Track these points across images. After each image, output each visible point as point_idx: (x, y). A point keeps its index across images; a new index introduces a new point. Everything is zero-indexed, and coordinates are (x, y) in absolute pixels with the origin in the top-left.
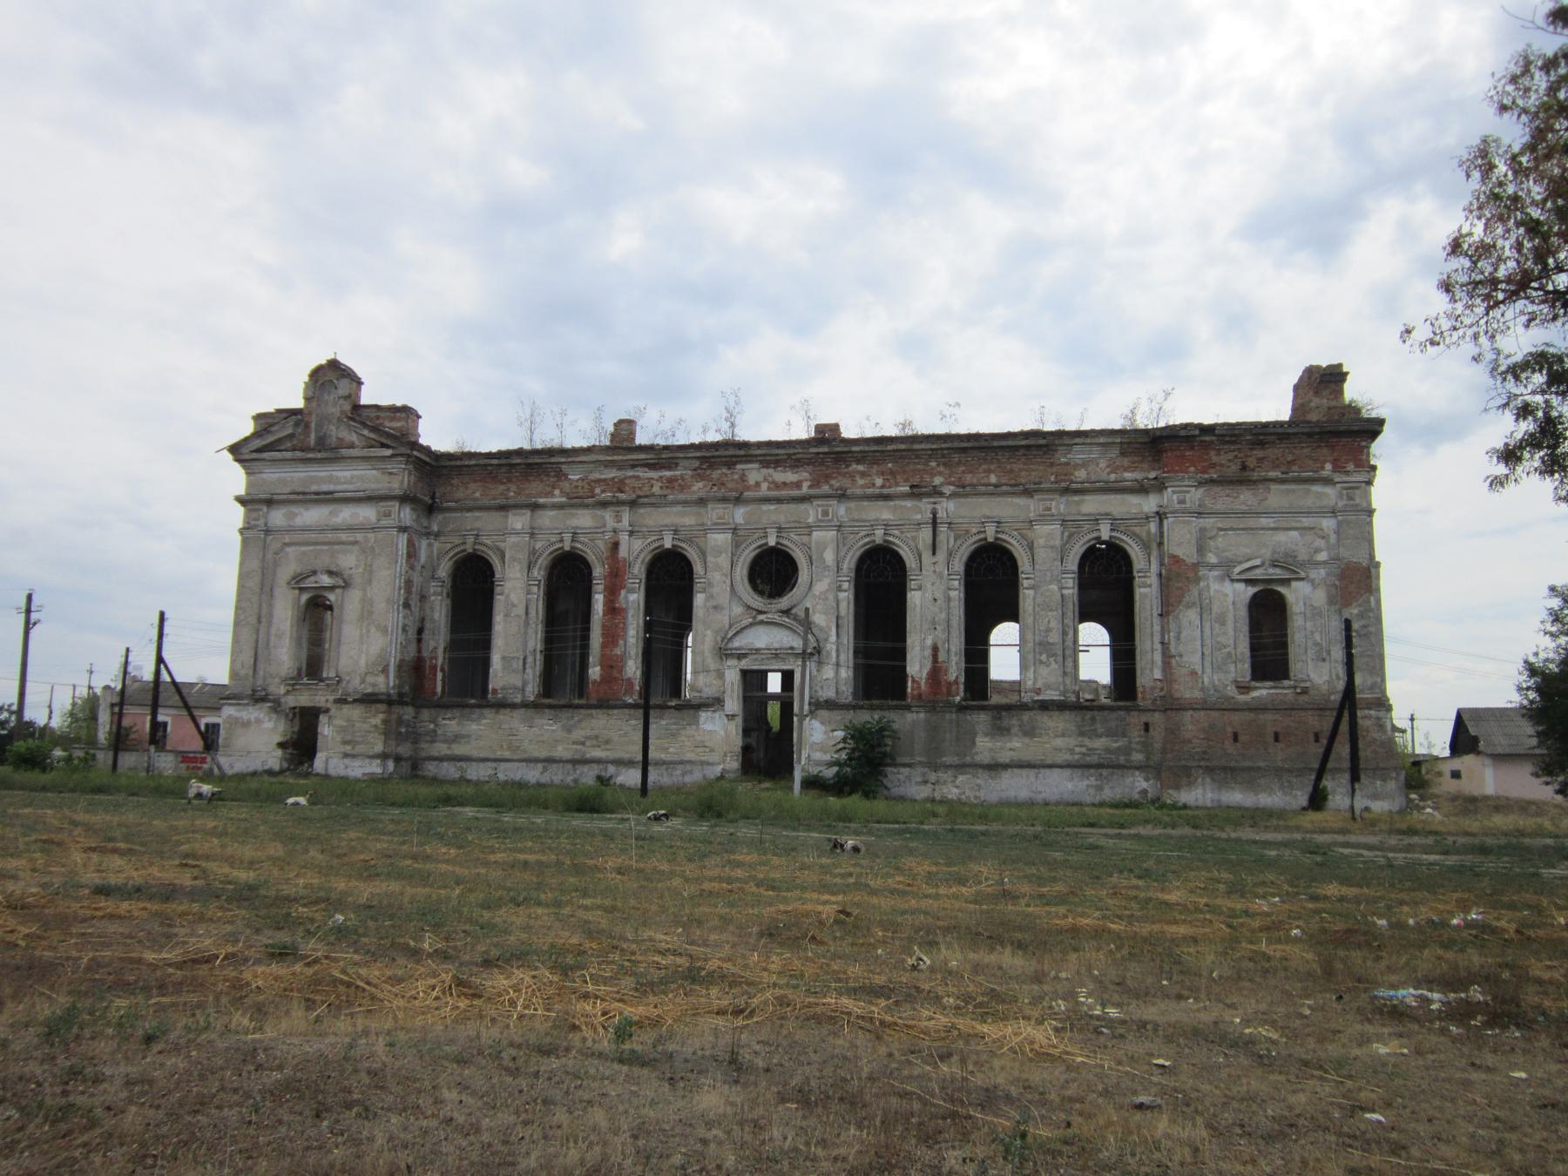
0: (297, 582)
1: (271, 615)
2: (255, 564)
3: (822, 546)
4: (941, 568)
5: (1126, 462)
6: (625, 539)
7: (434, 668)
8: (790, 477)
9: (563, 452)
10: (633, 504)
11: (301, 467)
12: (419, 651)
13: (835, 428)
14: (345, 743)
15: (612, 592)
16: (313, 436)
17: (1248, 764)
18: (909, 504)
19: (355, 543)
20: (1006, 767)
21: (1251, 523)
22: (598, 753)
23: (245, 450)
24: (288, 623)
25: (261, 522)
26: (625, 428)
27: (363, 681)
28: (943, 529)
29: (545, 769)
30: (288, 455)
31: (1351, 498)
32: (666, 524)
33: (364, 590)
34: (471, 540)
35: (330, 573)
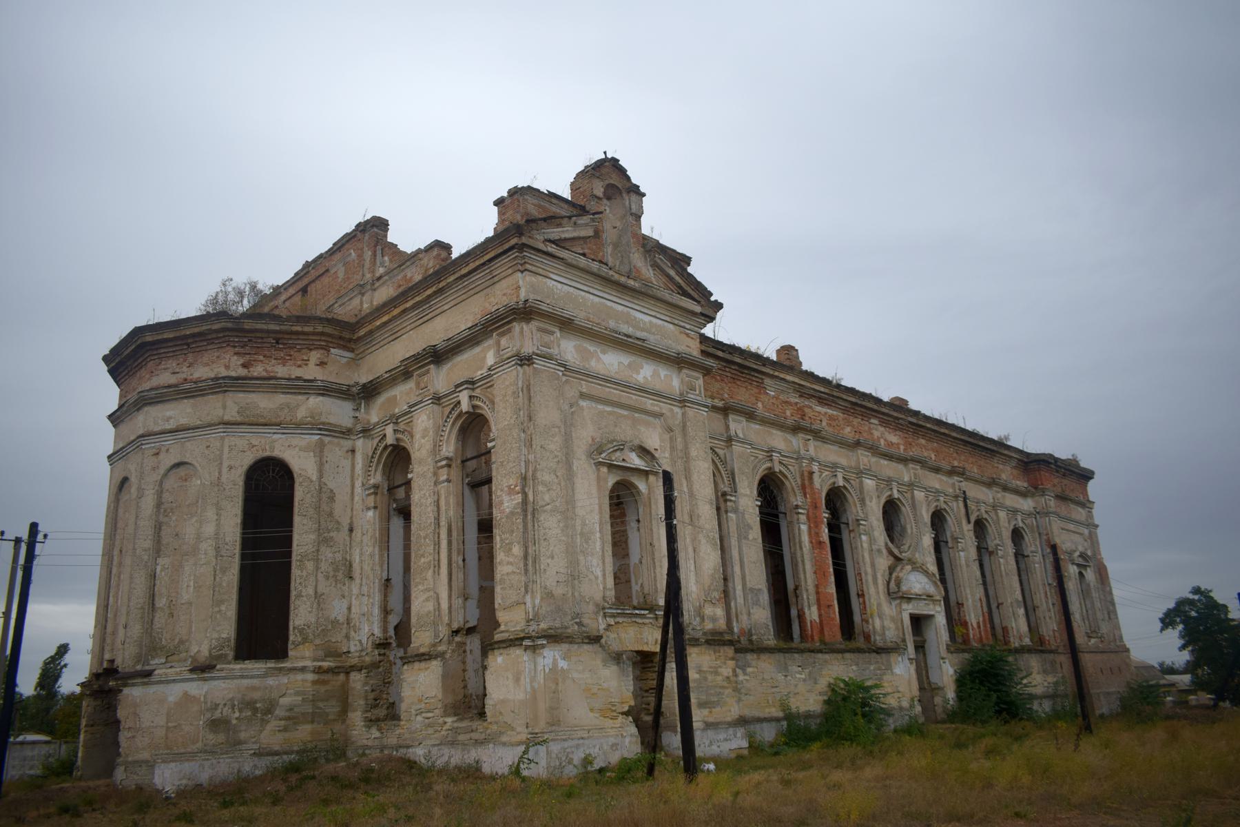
0: (603, 456)
5: (1015, 472)
8: (893, 438)
18: (944, 478)
19: (658, 415)
30: (583, 262)
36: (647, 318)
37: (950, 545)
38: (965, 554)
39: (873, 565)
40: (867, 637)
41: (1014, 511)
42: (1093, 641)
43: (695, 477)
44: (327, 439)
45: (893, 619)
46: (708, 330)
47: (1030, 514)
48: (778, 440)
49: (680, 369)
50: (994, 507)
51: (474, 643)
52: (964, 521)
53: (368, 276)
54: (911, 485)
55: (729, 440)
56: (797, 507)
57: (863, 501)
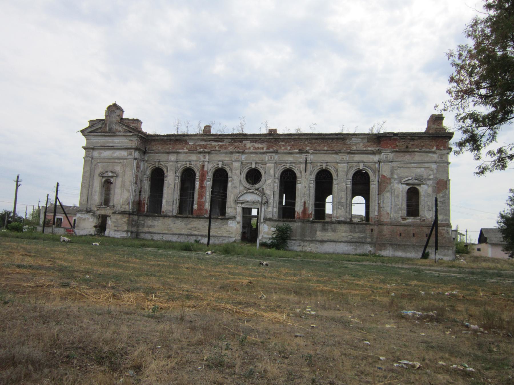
0: (102, 175)
1: (93, 185)
2: (88, 168)
3: (270, 168)
4: (308, 177)
5: (369, 144)
6: (206, 164)
7: (144, 204)
8: (260, 146)
9: (188, 135)
10: (209, 153)
11: (104, 138)
12: (140, 198)
13: (275, 130)
14: (115, 226)
15: (202, 181)
16: (108, 128)
17: (404, 243)
18: (298, 155)
19: (120, 163)
20: (326, 241)
21: (409, 165)
22: (196, 233)
23: (86, 132)
24: (98, 188)
25: (90, 155)
26: (208, 128)
27: (121, 207)
28: (309, 164)
29: (179, 237)
30: (99, 134)
31: (441, 158)
32: (219, 160)
33: (123, 178)
34: (157, 163)
35: (112, 172)
36: (118, 140)
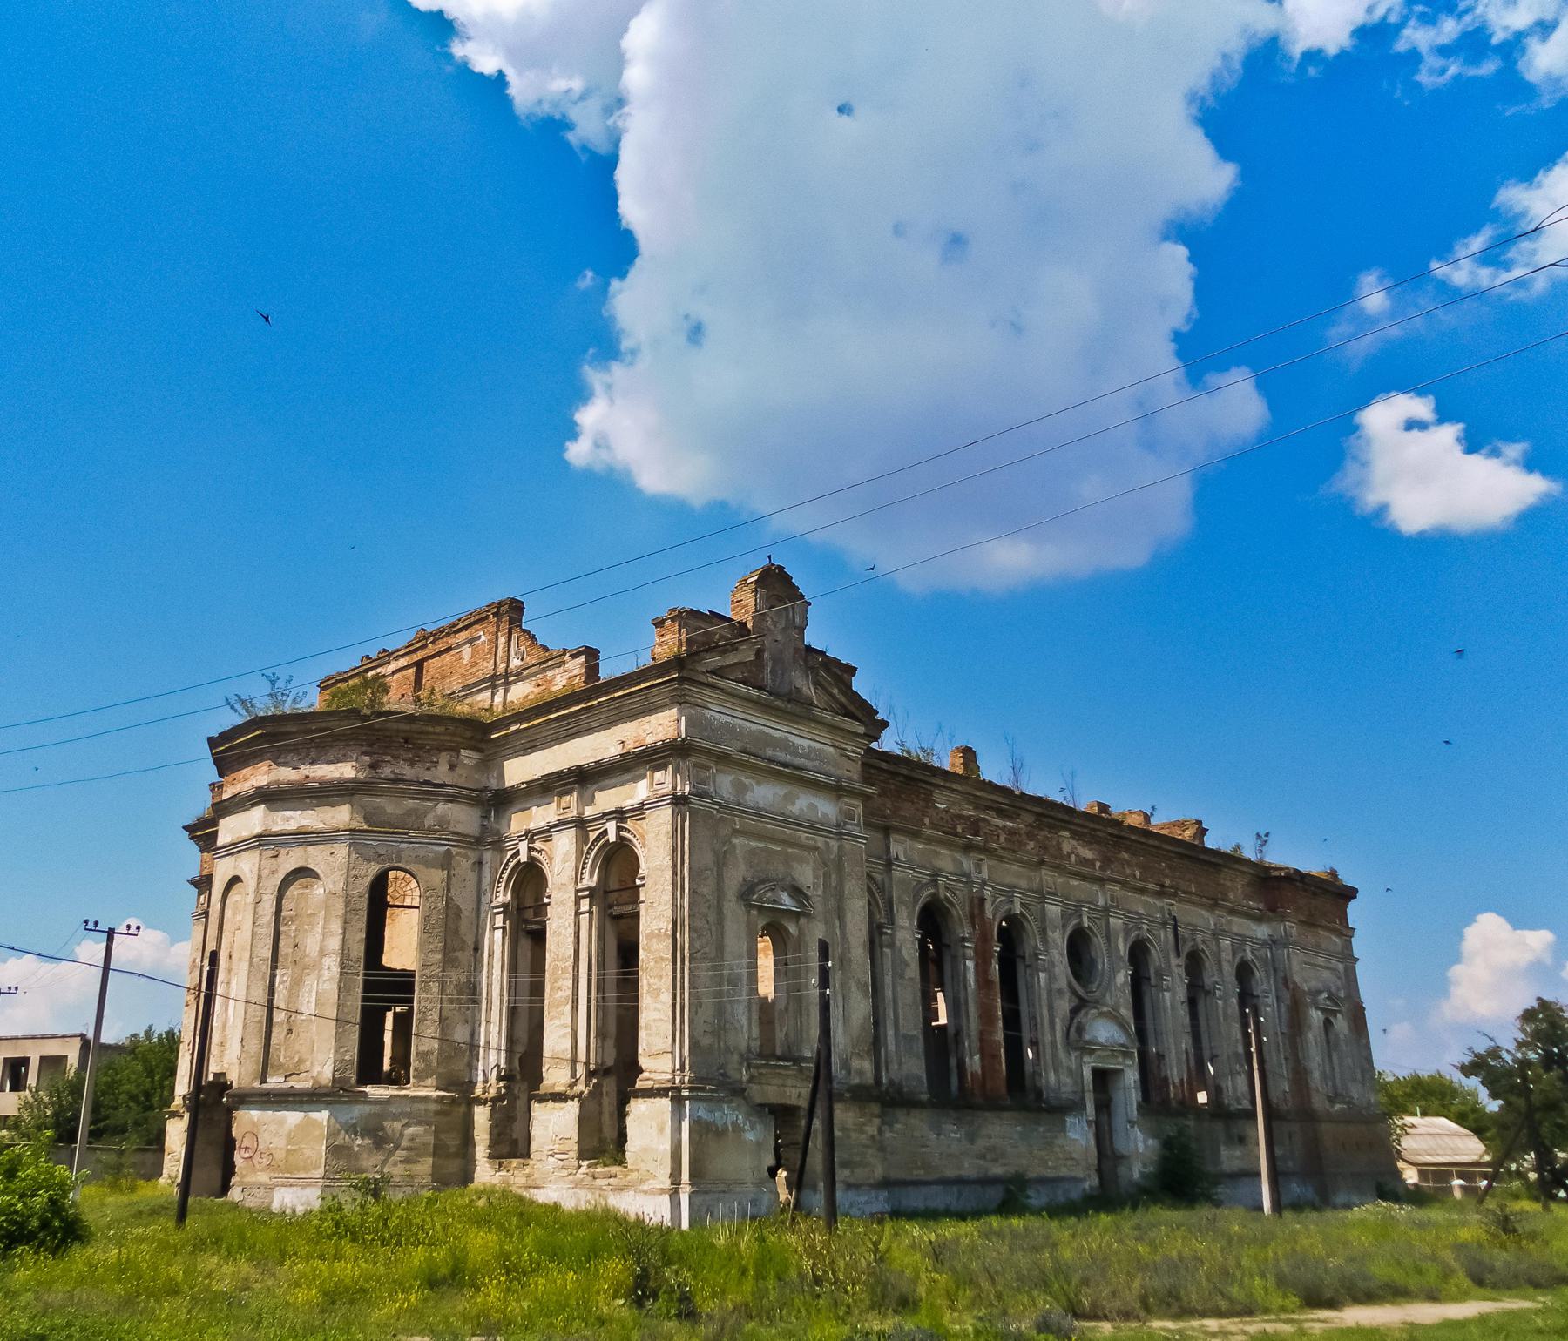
9: (927, 767)
18: (1150, 900)
36: (805, 743)
37: (1153, 982)
38: (1172, 996)
39: (1051, 1008)
40: (1039, 1093)
41: (1241, 941)
42: (1337, 1107)
43: (849, 916)
44: (454, 850)
45: (1070, 1072)
46: (874, 745)
47: (1264, 943)
48: (946, 860)
49: (839, 797)
50: (1215, 936)
51: (610, 1085)
52: (1172, 956)
53: (502, 667)
54: (1106, 910)
55: (889, 865)
56: (964, 939)
57: (1043, 932)
